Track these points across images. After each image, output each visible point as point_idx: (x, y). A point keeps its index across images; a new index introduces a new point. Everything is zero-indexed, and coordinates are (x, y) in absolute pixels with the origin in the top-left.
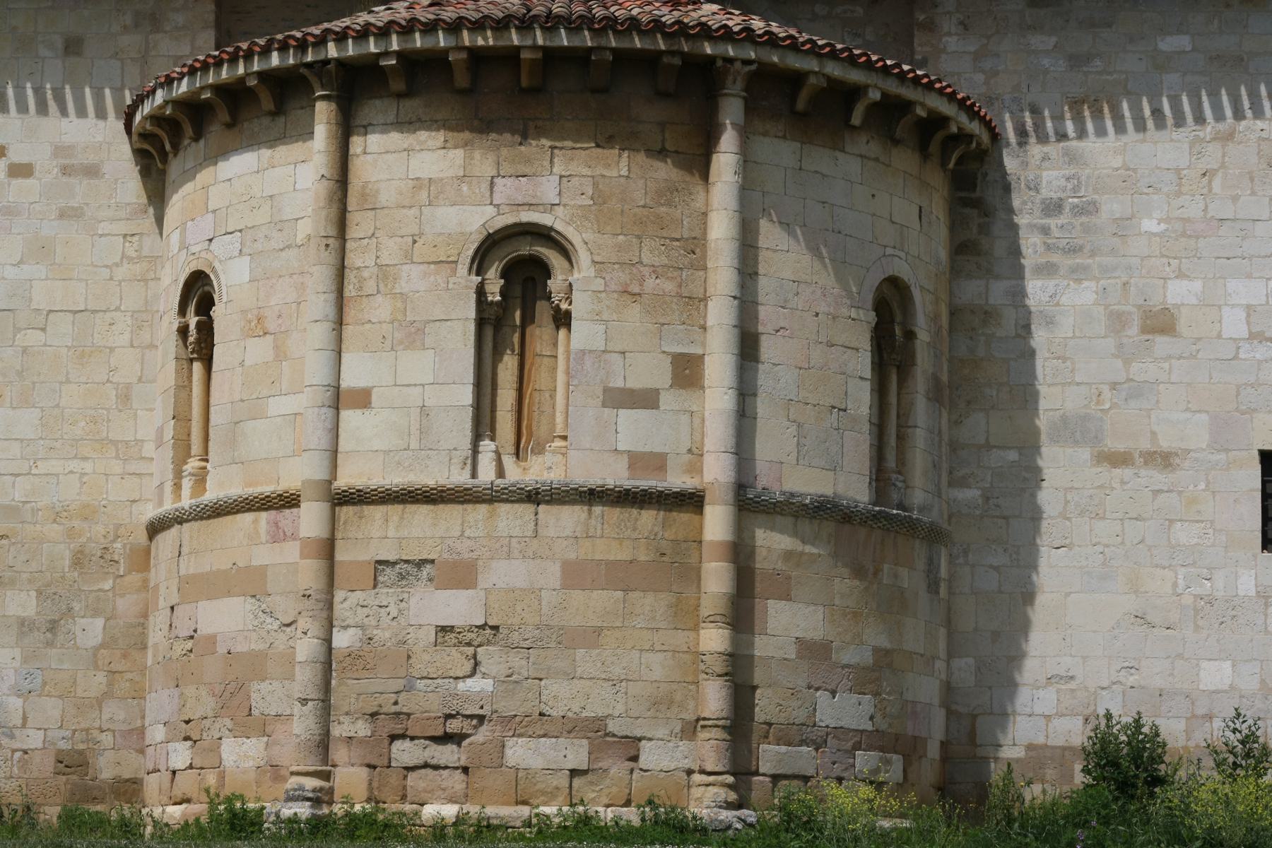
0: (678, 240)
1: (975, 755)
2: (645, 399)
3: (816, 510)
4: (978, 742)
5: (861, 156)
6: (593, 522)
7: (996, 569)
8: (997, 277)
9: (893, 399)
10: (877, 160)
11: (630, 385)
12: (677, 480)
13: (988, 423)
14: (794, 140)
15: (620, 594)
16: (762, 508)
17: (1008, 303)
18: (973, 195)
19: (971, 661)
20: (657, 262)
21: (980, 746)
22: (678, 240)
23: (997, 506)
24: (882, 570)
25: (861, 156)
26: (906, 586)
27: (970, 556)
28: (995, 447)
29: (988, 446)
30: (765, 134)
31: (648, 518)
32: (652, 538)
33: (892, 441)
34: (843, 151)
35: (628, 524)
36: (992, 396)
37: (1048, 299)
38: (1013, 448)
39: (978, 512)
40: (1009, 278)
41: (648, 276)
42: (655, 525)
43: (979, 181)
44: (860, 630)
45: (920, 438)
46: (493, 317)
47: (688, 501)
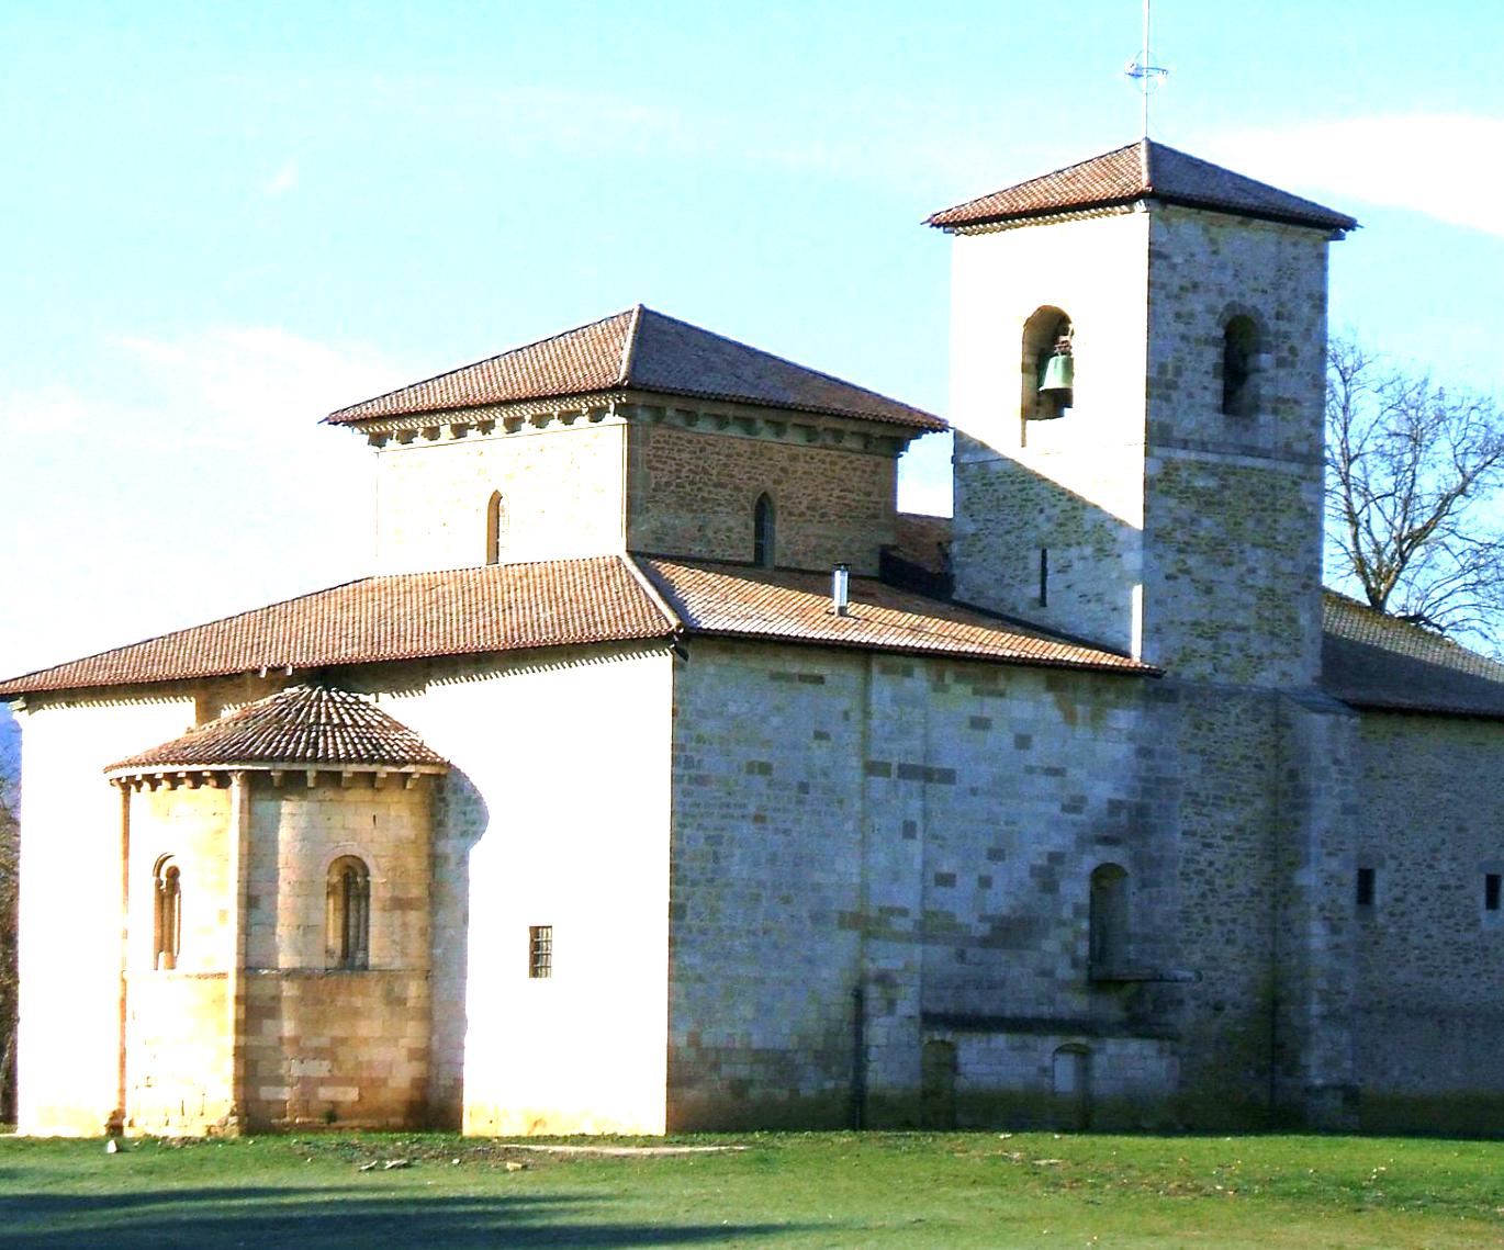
9: (362, 913)
30: (262, 799)
33: (362, 934)
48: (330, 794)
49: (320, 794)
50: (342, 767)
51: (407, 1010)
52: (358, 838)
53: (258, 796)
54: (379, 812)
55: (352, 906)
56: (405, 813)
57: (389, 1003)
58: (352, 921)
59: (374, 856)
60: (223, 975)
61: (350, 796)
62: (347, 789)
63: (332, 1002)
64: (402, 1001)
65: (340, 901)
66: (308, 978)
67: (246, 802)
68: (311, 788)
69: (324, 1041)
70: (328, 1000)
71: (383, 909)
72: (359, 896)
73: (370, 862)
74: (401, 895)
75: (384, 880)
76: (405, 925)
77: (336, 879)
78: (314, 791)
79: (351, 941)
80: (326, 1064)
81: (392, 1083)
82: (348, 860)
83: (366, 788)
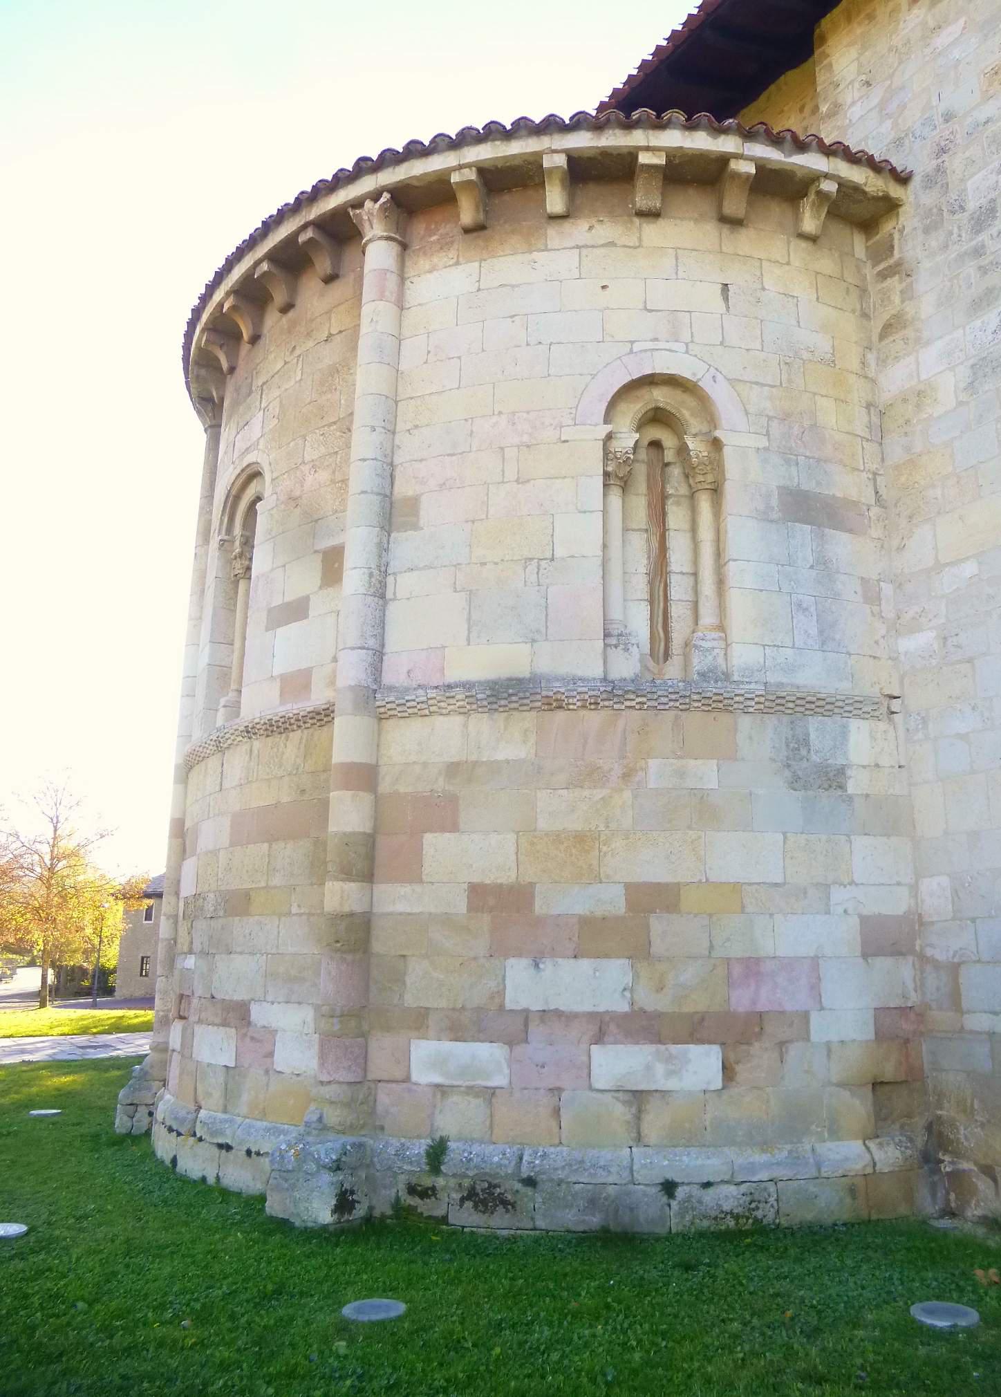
0: (335, 423)
1: (962, 1027)
2: (296, 611)
3: (491, 699)
4: (965, 1004)
5: (578, 247)
6: (252, 764)
7: (960, 736)
8: (928, 343)
9: (706, 533)
10: (612, 244)
11: (287, 599)
12: (318, 697)
13: (935, 536)
14: (469, 261)
15: (266, 845)
16: (410, 711)
17: (942, 368)
18: (891, 261)
19: (944, 880)
20: (315, 455)
21: (969, 1012)
22: (335, 423)
23: (958, 646)
24: (645, 770)
25: (578, 247)
26: (714, 784)
27: (931, 726)
28: (948, 564)
29: (939, 567)
31: (291, 747)
32: (294, 772)
34: (546, 250)
35: (276, 760)
36: (936, 498)
37: (990, 338)
38: (967, 558)
39: (934, 662)
40: (941, 337)
41: (308, 474)
42: (297, 757)
43: (896, 242)
44: (595, 862)
45: (741, 575)
46: (240, 572)
47: (325, 719)
48: (606, 230)
49: (579, 231)
50: (638, 138)
51: (850, 798)
52: (686, 336)
53: (424, 263)
54: (738, 276)
55: (676, 517)
56: (802, 289)
57: (795, 782)
58: (679, 558)
59: (730, 381)
60: (323, 716)
61: (652, 232)
62: (652, 215)
63: (626, 776)
64: (834, 778)
65: (640, 504)
66: (555, 704)
67: (392, 280)
68: (554, 218)
69: (611, 900)
70: (618, 770)
71: (764, 517)
72: (692, 496)
73: (719, 394)
74: (808, 485)
75: (763, 442)
76: (824, 566)
77: (627, 439)
78: (567, 226)
79: (679, 612)
80: (616, 972)
81: (822, 1029)
82: (660, 396)
83: (701, 218)
